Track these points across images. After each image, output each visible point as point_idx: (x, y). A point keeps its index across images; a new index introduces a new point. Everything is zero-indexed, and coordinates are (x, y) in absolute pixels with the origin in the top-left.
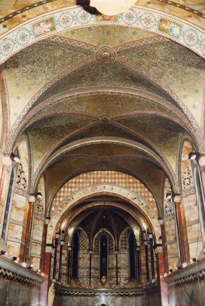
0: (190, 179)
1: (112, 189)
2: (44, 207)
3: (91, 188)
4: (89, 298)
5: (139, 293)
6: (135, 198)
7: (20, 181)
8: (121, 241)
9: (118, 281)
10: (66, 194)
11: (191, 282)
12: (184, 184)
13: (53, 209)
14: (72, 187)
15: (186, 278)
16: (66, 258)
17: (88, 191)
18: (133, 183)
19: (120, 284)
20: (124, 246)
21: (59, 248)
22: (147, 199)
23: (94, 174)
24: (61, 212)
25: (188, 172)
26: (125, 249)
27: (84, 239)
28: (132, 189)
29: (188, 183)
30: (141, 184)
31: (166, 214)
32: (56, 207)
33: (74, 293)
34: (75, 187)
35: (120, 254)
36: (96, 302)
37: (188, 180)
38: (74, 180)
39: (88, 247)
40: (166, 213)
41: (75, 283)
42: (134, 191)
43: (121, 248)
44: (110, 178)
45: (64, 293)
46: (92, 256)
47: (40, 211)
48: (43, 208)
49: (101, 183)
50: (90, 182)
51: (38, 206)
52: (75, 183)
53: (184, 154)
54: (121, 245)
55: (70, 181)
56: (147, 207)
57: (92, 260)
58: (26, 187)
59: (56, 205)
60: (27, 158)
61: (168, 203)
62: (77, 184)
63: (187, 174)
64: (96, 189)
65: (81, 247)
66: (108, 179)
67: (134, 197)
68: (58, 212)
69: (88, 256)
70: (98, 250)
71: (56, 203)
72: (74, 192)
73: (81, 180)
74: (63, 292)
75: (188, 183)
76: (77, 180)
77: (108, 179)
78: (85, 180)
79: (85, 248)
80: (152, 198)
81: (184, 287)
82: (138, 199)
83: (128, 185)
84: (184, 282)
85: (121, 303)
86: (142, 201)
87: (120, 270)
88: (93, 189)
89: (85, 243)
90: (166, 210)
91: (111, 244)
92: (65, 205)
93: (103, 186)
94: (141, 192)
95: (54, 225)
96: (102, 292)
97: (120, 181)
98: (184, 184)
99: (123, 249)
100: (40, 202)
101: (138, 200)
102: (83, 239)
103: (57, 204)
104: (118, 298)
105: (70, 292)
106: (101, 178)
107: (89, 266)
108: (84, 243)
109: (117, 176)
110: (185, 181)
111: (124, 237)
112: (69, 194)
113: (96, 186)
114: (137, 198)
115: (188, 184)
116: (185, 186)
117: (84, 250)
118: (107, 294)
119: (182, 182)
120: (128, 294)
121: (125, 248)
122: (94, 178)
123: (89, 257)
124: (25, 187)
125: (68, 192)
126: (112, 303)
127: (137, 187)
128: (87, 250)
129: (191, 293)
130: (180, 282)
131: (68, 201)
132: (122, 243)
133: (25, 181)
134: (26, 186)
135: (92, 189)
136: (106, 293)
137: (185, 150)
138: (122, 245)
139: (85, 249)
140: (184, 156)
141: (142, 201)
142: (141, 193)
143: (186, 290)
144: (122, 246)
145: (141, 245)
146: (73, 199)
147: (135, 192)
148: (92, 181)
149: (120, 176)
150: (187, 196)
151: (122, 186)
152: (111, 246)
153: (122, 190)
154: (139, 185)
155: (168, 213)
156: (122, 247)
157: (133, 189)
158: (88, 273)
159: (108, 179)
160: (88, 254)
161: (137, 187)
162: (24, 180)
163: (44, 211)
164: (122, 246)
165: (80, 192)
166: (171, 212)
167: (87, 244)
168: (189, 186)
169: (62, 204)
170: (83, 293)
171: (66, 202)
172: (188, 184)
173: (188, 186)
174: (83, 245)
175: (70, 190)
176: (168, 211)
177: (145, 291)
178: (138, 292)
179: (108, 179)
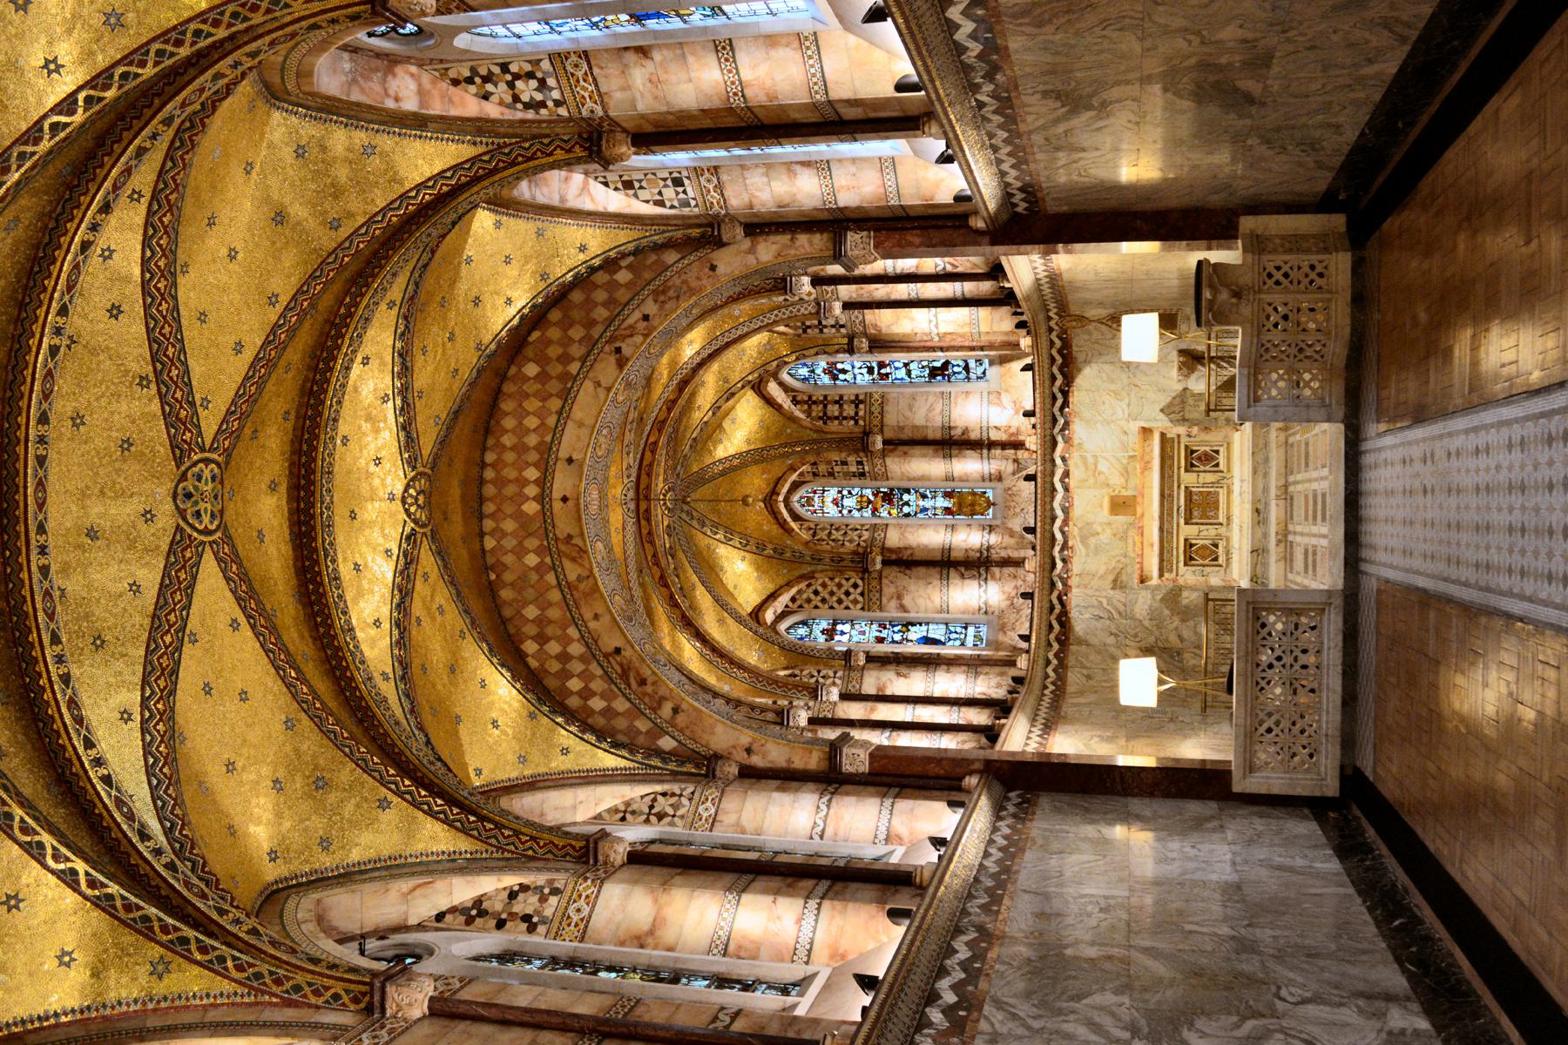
0: (517, 77)
1: (570, 461)
2: (659, 788)
3: (567, 564)
4: (1076, 567)
5: (1058, 343)
6: (618, 350)
7: (527, 918)
9: (1002, 437)
10: (597, 685)
11: (1009, 99)
12: (543, 104)
13: (667, 743)
14: (564, 657)
15: (989, 120)
16: (899, 674)
17: (579, 579)
18: (542, 361)
19: (1018, 432)
20: (849, 410)
21: (855, 711)
22: (622, 295)
23: (499, 548)
24: (684, 706)
25: (478, 80)
27: (816, 593)
28: (574, 368)
29: (533, 83)
30: (549, 323)
31: (693, 203)
32: (658, 731)
33: (1052, 636)
34: (566, 641)
36: (1092, 541)
37: (519, 84)
38: (530, 647)
40: (688, 205)
42: (584, 360)
43: (856, 422)
44: (521, 470)
45: (1053, 683)
46: (894, 557)
47: (675, 807)
48: (664, 794)
49: (546, 514)
50: (537, 568)
51: (653, 819)
52: (542, 639)
53: (387, 95)
55: (533, 663)
56: (662, 298)
58: (557, 885)
59: (648, 732)
60: (405, 885)
61: (644, 194)
62: (549, 631)
63: (489, 87)
64: (574, 541)
66: (524, 482)
67: (612, 359)
68: (681, 719)
69: (892, 572)
71: (639, 732)
72: (587, 644)
73: (531, 612)
74: (1052, 688)
75: (533, 83)
76: (531, 630)
77: (526, 482)
78: (530, 593)
80: (615, 272)
81: (1030, 132)
82: (624, 338)
83: (554, 386)
84: (1006, 135)
85: (1099, 426)
86: (631, 321)
88: (574, 554)
90: (676, 203)
91: (837, 469)
92: (649, 689)
93: (557, 505)
94: (592, 323)
95: (745, 738)
96: (1052, 509)
97: (532, 422)
98: (543, 104)
99: (861, 413)
100: (634, 807)
101: (629, 341)
103: (642, 725)
104: (1076, 442)
105: (1051, 656)
106: (519, 516)
109: (507, 440)
110: (525, 98)
112: (599, 672)
113: (557, 539)
114: (618, 344)
115: (542, 84)
116: (550, 104)
118: (1058, 486)
119: (530, 115)
120: (1059, 395)
122: (520, 552)
124: (555, 891)
125: (586, 676)
126: (1101, 467)
127: (567, 342)
129: (1052, 104)
130: (1009, 154)
131: (632, 675)
133: (524, 888)
134: (550, 882)
135: (573, 560)
136: (1054, 490)
137: (362, 90)
138: (841, 418)
139: (859, 590)
140: (397, 100)
141: (631, 321)
142: (592, 323)
143: (1044, 128)
145: (843, 330)
146: (618, 651)
147: (588, 354)
148: (532, 560)
149: (509, 423)
150: (600, 95)
151: (560, 413)
153: (577, 413)
154: (554, 333)
155: (691, 194)
157: (574, 359)
158: (966, 574)
159: (526, 482)
161: (567, 342)
162: (521, 896)
163: (676, 788)
165: (588, 615)
166: (686, 182)
168: (551, 82)
169: (647, 700)
170: (1055, 594)
171: (632, 681)
172: (542, 84)
173: (551, 89)
175: (576, 667)
176: (682, 196)
177: (1050, 318)
178: (1054, 352)
179: (524, 482)
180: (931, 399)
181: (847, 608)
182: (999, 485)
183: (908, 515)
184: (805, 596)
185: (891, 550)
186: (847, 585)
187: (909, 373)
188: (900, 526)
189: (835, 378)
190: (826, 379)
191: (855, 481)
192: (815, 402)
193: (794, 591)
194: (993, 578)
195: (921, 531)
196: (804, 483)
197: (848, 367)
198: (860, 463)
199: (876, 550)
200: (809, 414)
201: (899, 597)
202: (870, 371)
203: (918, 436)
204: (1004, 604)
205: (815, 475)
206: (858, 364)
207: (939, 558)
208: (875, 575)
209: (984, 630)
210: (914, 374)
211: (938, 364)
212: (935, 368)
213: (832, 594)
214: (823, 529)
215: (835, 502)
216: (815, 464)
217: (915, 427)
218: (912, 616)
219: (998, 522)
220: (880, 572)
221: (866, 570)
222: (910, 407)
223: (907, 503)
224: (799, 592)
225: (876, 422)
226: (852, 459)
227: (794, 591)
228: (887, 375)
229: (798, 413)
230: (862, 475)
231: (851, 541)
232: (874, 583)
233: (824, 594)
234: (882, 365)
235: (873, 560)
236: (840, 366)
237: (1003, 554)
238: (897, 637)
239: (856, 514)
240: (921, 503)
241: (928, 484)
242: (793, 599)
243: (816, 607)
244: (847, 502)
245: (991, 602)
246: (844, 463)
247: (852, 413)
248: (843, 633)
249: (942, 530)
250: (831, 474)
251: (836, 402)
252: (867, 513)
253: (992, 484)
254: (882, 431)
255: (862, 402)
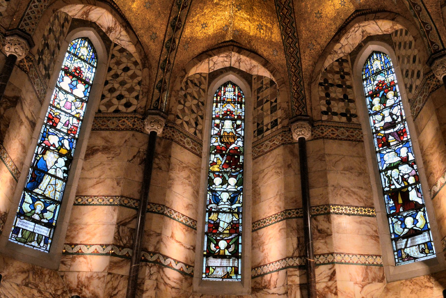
8: (320, 84)
20: (337, 107)
26: (344, 119)
27: (126, 69)
35: (320, 141)
39: (143, 103)
41: (20, 279)
46: (159, 149)
54: (323, 102)
57: (160, 168)
65: (105, 100)
70: (195, 133)
79: (128, 105)
87: (329, 221)
89: (128, 86)
99: (336, 118)
102: (122, 66)
107: (137, 196)
108: (123, 83)
111: (338, 70)
117: (118, 115)
121: (343, 115)
123: (145, 147)
128: (135, 111)
132: (328, 95)
144: (328, 103)
152: (269, 112)
156: (329, 109)
160: (139, 135)
164: (328, 103)
167: (138, 88)
174: (117, 93)
180: (363, 193)
181: (103, 97)
182: (247, 289)
183: (211, 182)
184: (124, 60)
185: (168, 148)
186: (131, 97)
187: (395, 166)
188: (198, 169)
189: (373, 95)
190: (369, 88)
191: (252, 128)
192: (342, 77)
193: (131, 49)
194: (112, 265)
195: (189, 190)
196: (250, 83)
197: (389, 103)
198: (275, 123)
199: (169, 133)
200: (330, 70)
201: (106, 149)
202: (393, 125)
203: (313, 177)
204: (73, 279)
205: (259, 90)
206: (396, 111)
207: (152, 198)
208: (138, 125)
209: (43, 248)
210: (395, 173)
211: (413, 196)
212: (406, 195)
213: (123, 83)
214: (199, 93)
215: (227, 115)
216: (272, 82)
217: (324, 173)
218: (80, 163)
219: (196, 287)
220: (141, 131)
221: (145, 115)
222: (350, 169)
223: (225, 182)
224: (130, 55)
225: (327, 132)
226: (279, 113)
227: (131, 49)
228: (387, 145)
229: (329, 61)
230: (260, 131)
231: (183, 111)
232: (129, 123)
233: (124, 76)
234: (400, 134)
235: (157, 122)
236: (390, 95)
237: (149, 284)
238: (53, 140)
239: (215, 131)
240: (225, 197)
241: (249, 202)
242: (122, 50)
243: (110, 69)
244: (228, 124)
245: (81, 259)
246: (273, 110)
247: (335, 110)
248: (73, 87)
249: (187, 213)
250: (260, 103)
251: (345, 97)
252: (215, 142)
253: (248, 280)
254: (315, 138)
255: (349, 120)
